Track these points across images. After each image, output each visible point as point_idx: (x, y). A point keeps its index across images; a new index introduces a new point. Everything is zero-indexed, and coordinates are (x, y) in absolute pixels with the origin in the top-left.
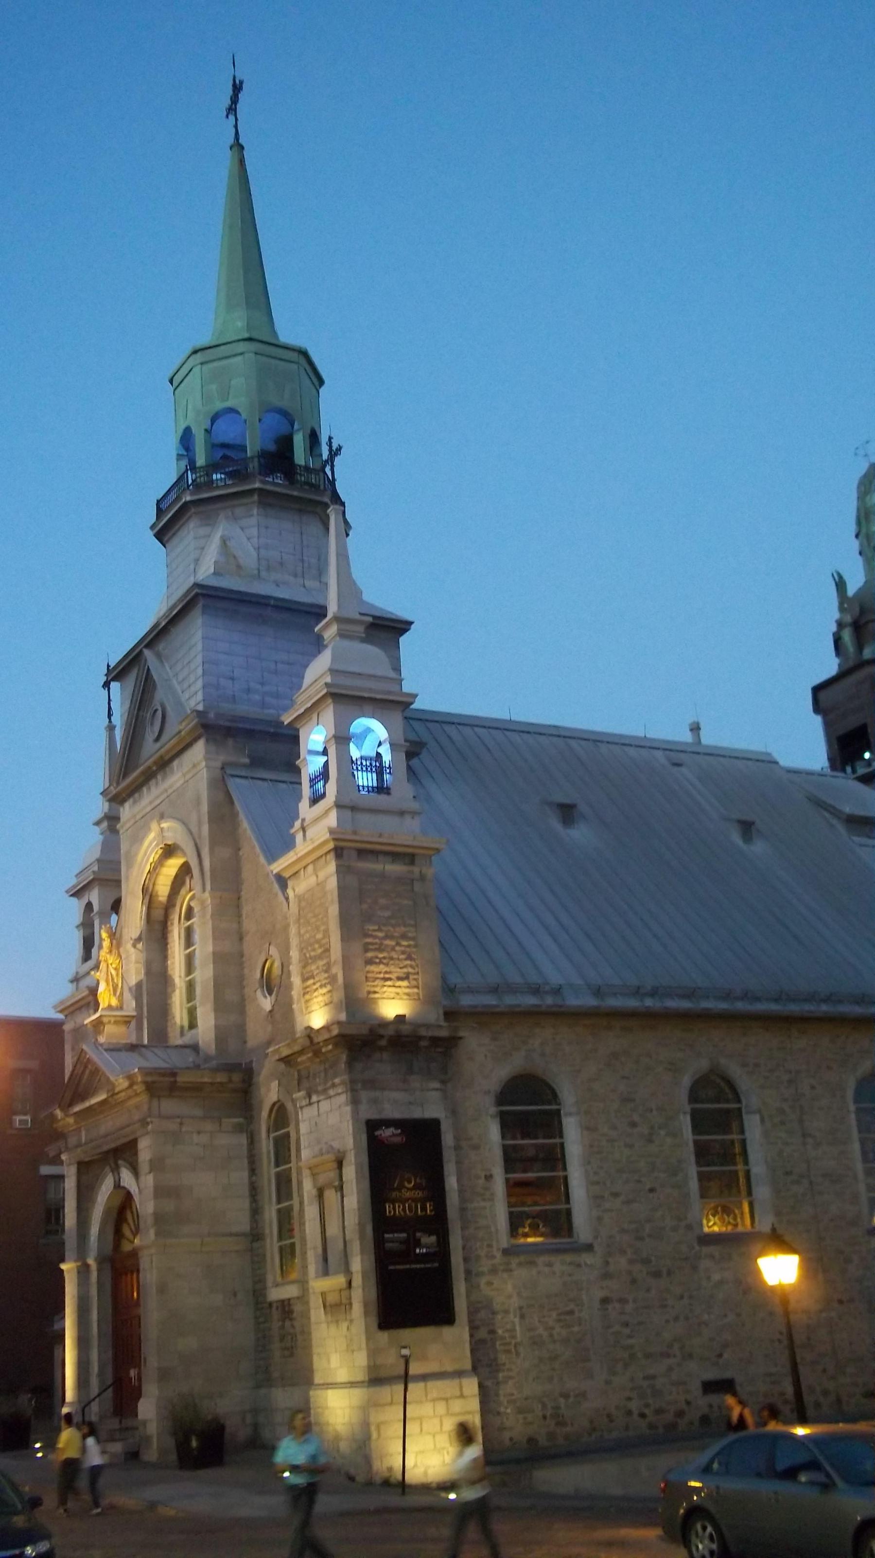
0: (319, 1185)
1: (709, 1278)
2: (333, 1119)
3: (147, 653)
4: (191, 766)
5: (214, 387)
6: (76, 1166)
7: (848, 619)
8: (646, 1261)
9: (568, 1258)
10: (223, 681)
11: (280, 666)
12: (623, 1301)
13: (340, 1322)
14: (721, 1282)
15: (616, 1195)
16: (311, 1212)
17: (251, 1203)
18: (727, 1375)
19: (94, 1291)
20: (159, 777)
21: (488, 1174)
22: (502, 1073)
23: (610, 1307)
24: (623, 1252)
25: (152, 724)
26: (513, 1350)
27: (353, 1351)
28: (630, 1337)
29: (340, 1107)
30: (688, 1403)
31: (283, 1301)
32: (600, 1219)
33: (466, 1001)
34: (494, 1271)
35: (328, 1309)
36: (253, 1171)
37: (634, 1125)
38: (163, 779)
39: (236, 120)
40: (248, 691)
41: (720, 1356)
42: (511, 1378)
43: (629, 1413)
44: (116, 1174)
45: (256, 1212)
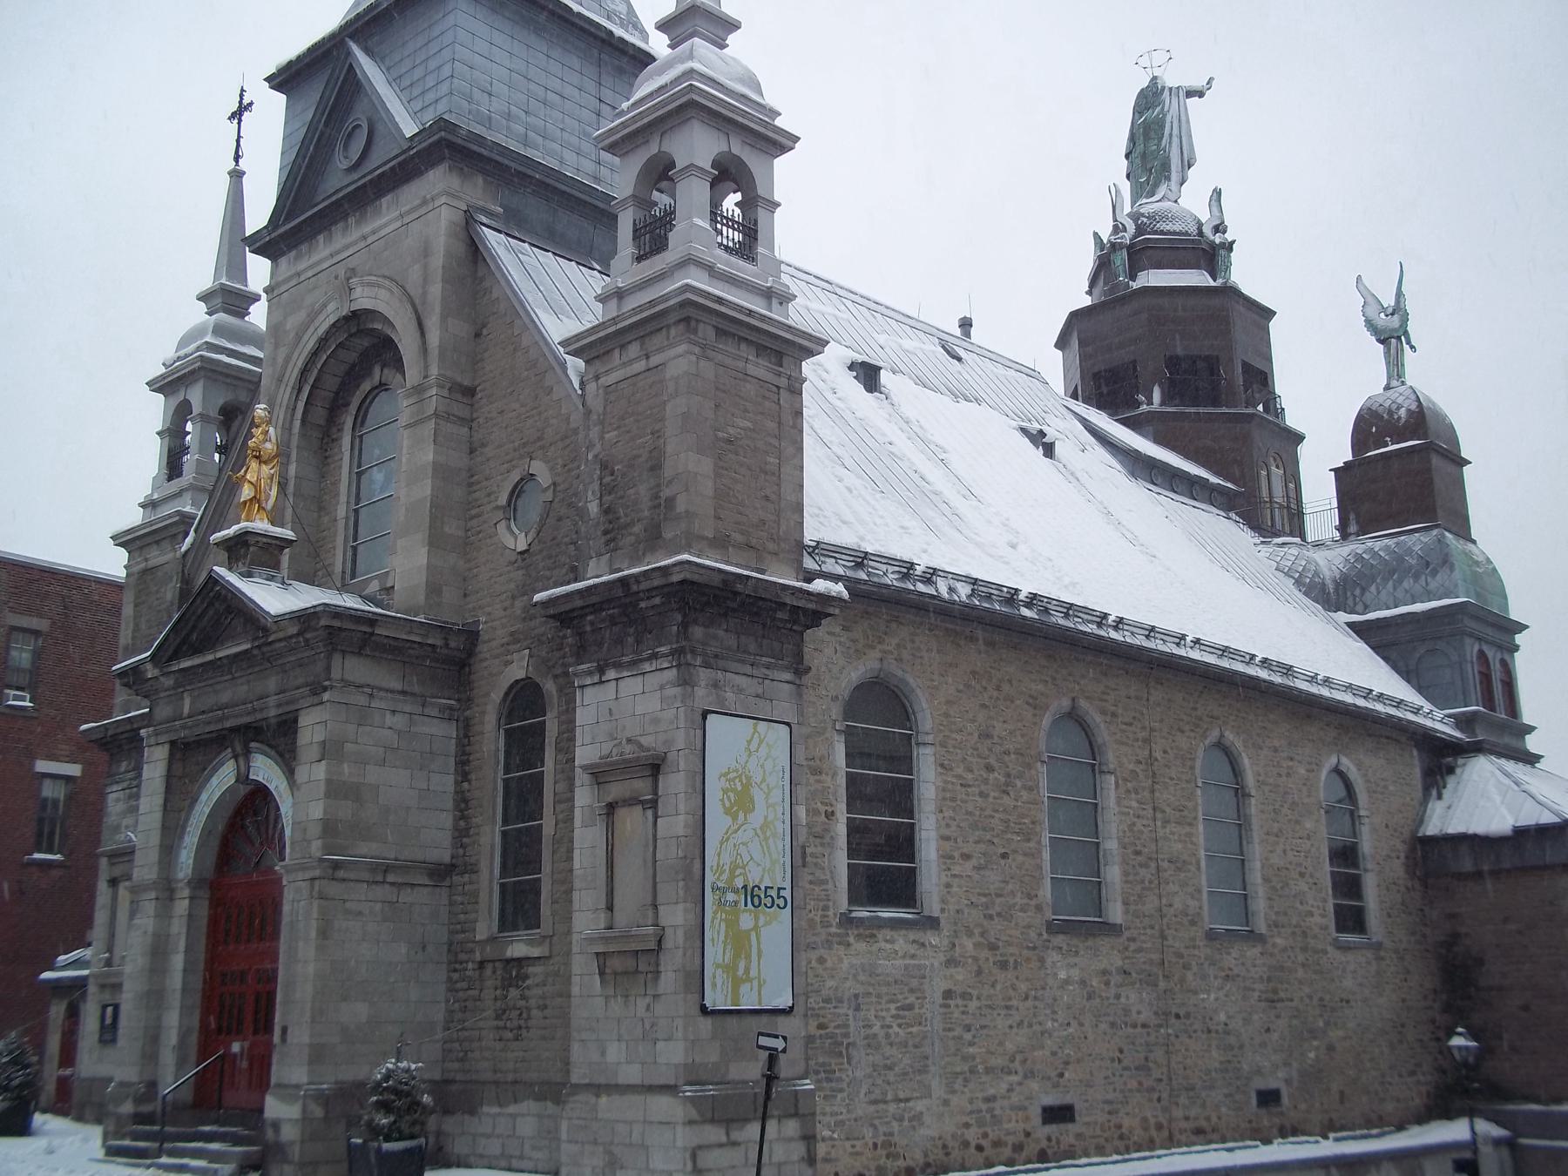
0: (610, 799)
1: (1056, 974)
2: (651, 704)
4: (417, 202)
6: (167, 746)
8: (993, 947)
9: (912, 935)
10: (477, 94)
11: (551, 96)
12: (966, 996)
13: (632, 999)
14: (1067, 982)
15: (966, 857)
16: (587, 839)
17: (456, 820)
18: (1067, 1099)
19: (178, 927)
20: (351, 220)
22: (855, 674)
23: (952, 1003)
24: (970, 934)
25: (346, 147)
26: (844, 1052)
28: (971, 1044)
29: (662, 688)
30: (1028, 1134)
32: (948, 886)
34: (828, 944)
37: (990, 768)
38: (358, 223)
40: (509, 116)
41: (1061, 1075)
42: (841, 1090)
43: (966, 1144)
45: (463, 832)
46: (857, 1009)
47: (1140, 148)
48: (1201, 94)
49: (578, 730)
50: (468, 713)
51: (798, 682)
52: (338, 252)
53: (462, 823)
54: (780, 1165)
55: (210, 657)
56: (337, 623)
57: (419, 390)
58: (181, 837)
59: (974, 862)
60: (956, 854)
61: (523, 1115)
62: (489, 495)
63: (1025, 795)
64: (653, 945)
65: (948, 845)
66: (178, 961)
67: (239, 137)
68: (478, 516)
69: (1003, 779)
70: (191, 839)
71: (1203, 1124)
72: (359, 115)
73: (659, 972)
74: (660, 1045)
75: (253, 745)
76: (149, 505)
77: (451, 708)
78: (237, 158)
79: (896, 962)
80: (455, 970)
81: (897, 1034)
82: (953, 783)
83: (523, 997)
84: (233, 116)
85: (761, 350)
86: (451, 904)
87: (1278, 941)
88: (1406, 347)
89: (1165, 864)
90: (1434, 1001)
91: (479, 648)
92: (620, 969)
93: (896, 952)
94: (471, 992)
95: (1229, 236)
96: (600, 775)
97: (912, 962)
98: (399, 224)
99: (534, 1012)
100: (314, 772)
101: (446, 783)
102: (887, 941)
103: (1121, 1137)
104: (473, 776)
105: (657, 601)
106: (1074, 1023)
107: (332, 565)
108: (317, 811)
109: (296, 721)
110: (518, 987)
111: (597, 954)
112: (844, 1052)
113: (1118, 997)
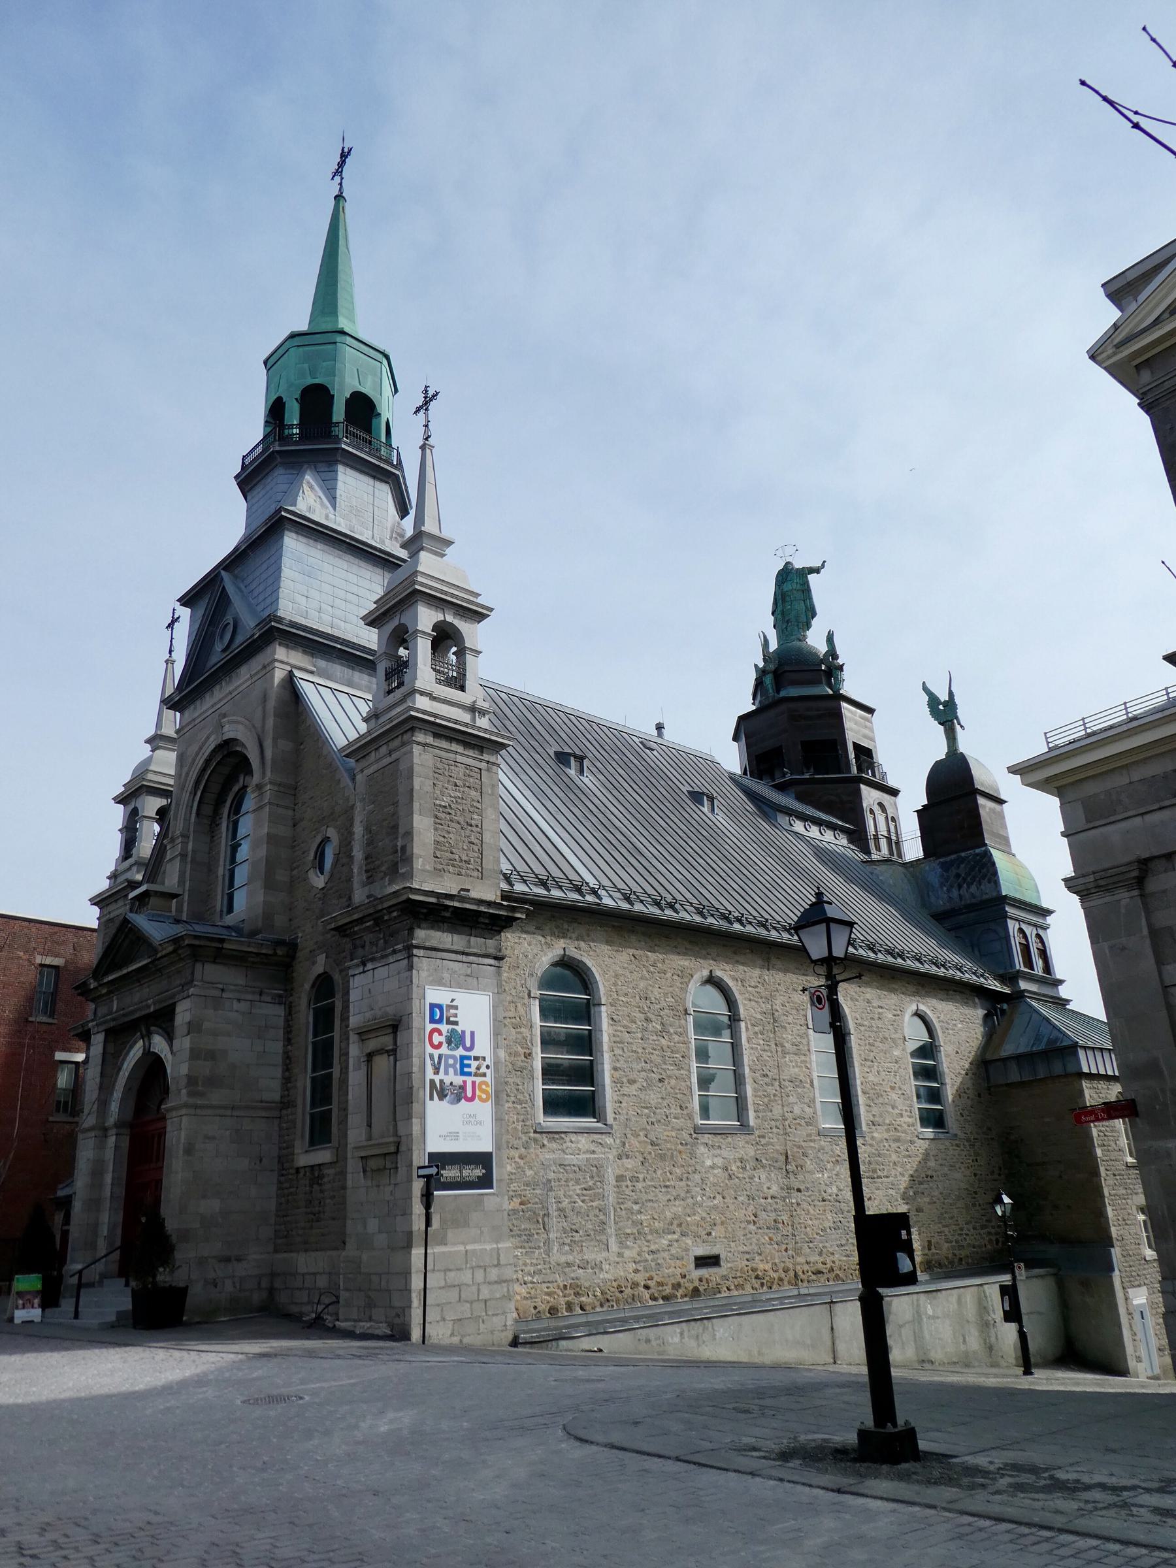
3: (223, 573)
4: (260, 667)
5: (306, 366)
7: (772, 667)
11: (350, 597)
13: (382, 1188)
14: (712, 1167)
16: (356, 1078)
17: (284, 1071)
19: (109, 1154)
21: (527, 1051)
25: (222, 637)
26: (540, 1220)
27: (395, 1216)
30: (684, 1276)
31: (312, 1167)
33: (520, 887)
35: (369, 1174)
36: (288, 1041)
39: (342, 179)
41: (709, 1234)
42: (539, 1247)
43: (635, 1285)
44: (146, 1039)
45: (287, 1081)
46: (551, 1189)
47: (780, 608)
48: (817, 571)
49: (351, 1005)
50: (291, 999)
51: (497, 964)
52: (215, 704)
53: (287, 1073)
54: (486, 1301)
55: (125, 971)
56: (197, 942)
57: (259, 787)
58: (112, 1094)
59: (638, 1085)
60: (625, 1080)
61: (321, 1274)
62: (304, 853)
63: (676, 1038)
64: (392, 1149)
65: (617, 1074)
66: (108, 1178)
67: (172, 638)
68: (298, 867)
69: (659, 1027)
70: (117, 1094)
71: (820, 1267)
72: (229, 618)
73: (397, 1168)
74: (398, 1218)
75: (153, 1028)
76: (113, 876)
77: (280, 996)
78: (170, 652)
79: (580, 1157)
80: (283, 1175)
81: (581, 1207)
82: (621, 1032)
83: (322, 1191)
84: (169, 626)
85: (467, 745)
86: (281, 1129)
87: (875, 1135)
88: (958, 727)
89: (787, 1083)
90: (1000, 1175)
91: (298, 955)
92: (374, 1168)
93: (579, 1150)
94: (291, 1190)
95: (840, 661)
96: (364, 1034)
97: (592, 1156)
98: (250, 682)
99: (328, 1201)
100: (184, 1043)
101: (277, 1047)
102: (571, 1142)
103: (757, 1277)
104: (293, 1041)
105: (395, 914)
106: (719, 1197)
107: (215, 906)
108: (184, 1069)
109: (174, 1010)
110: (318, 1184)
111: (362, 1157)
112: (540, 1220)
113: (752, 1178)
